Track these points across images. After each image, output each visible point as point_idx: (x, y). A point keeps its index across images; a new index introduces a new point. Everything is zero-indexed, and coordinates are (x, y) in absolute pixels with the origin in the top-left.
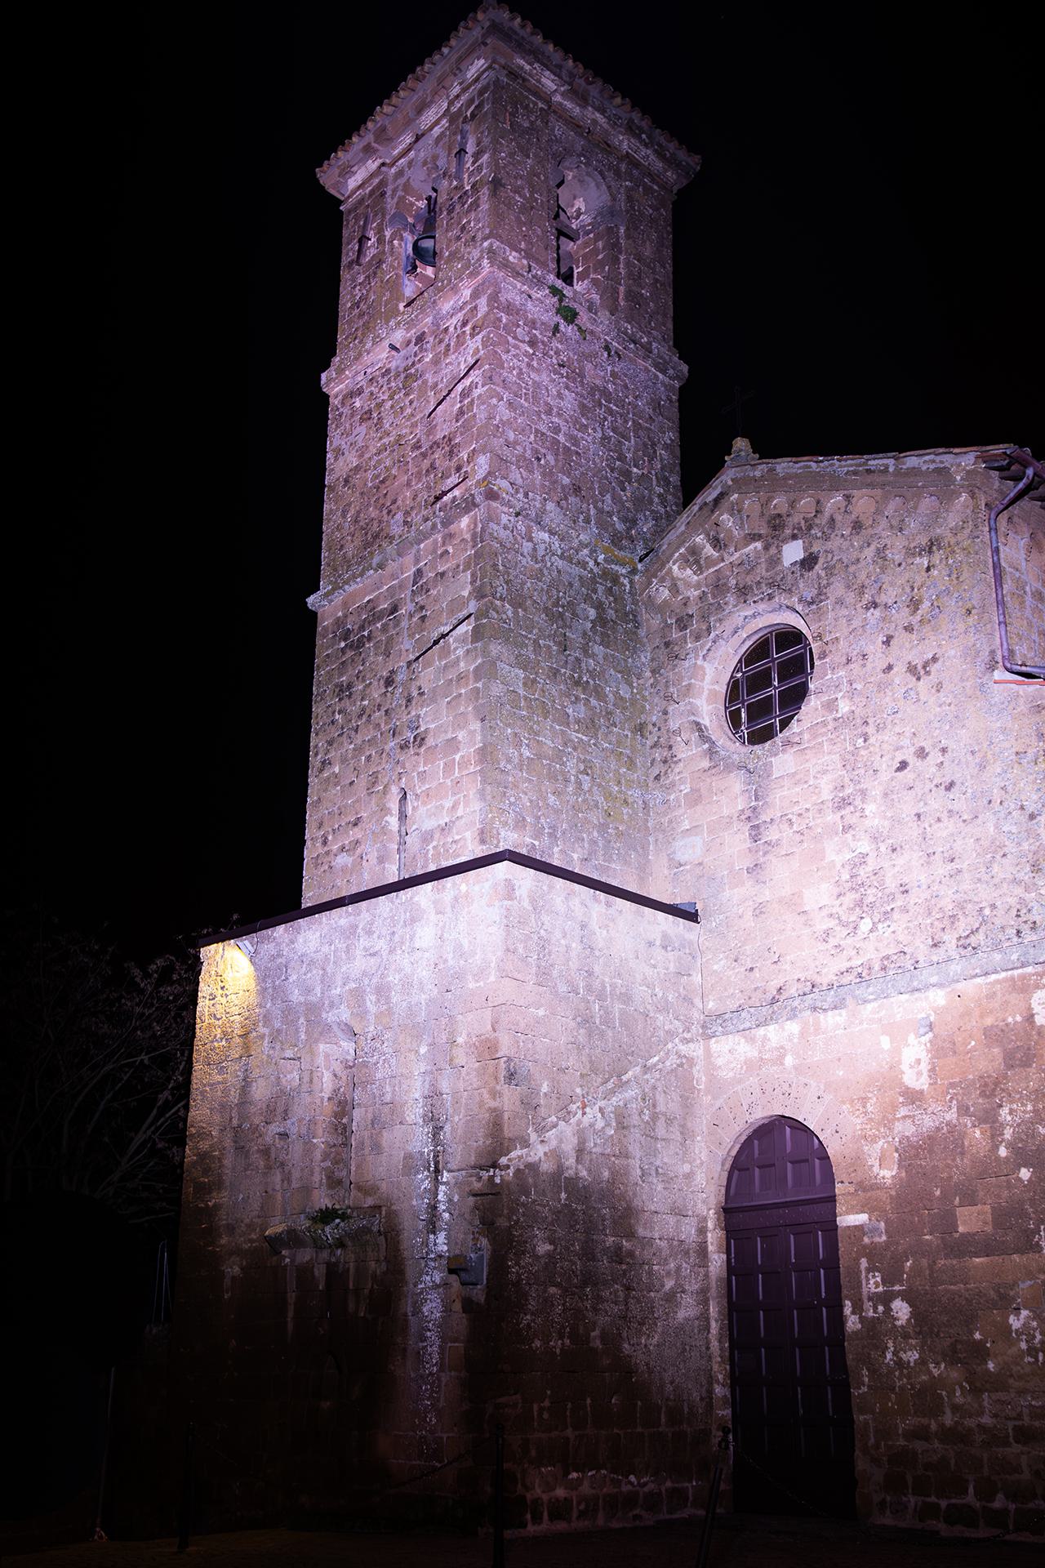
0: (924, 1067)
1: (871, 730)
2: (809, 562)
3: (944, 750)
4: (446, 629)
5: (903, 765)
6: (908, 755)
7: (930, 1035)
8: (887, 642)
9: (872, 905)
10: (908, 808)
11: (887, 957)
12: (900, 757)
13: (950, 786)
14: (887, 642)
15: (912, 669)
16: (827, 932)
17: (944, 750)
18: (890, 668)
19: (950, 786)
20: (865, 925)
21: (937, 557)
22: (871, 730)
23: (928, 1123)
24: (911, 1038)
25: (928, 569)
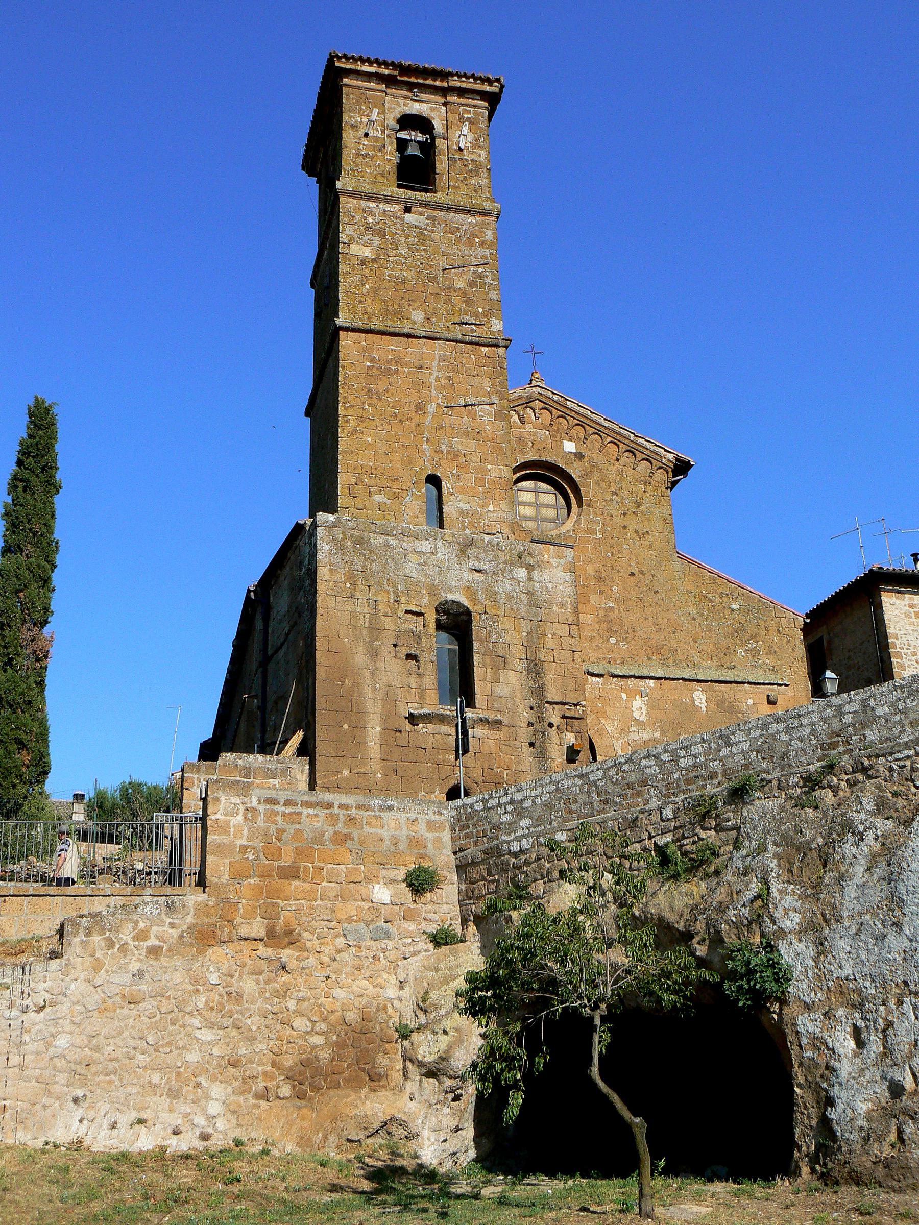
0: (644, 711)
1: (615, 551)
2: (579, 456)
3: (653, 576)
4: (470, 401)
5: (632, 574)
6: (636, 571)
7: (647, 698)
8: (625, 514)
9: (616, 632)
10: (634, 593)
11: (624, 658)
12: (631, 570)
13: (656, 592)
14: (625, 514)
15: (637, 533)
16: (592, 638)
17: (653, 576)
18: (625, 527)
19: (656, 592)
20: (613, 640)
21: (649, 488)
22: (615, 551)
23: (646, 736)
24: (637, 697)
25: (644, 491)
